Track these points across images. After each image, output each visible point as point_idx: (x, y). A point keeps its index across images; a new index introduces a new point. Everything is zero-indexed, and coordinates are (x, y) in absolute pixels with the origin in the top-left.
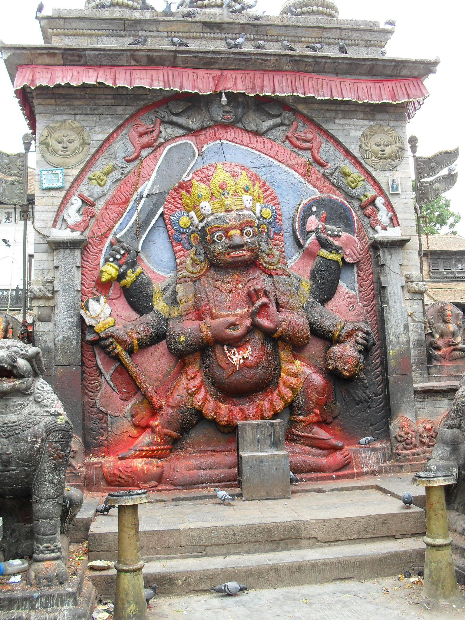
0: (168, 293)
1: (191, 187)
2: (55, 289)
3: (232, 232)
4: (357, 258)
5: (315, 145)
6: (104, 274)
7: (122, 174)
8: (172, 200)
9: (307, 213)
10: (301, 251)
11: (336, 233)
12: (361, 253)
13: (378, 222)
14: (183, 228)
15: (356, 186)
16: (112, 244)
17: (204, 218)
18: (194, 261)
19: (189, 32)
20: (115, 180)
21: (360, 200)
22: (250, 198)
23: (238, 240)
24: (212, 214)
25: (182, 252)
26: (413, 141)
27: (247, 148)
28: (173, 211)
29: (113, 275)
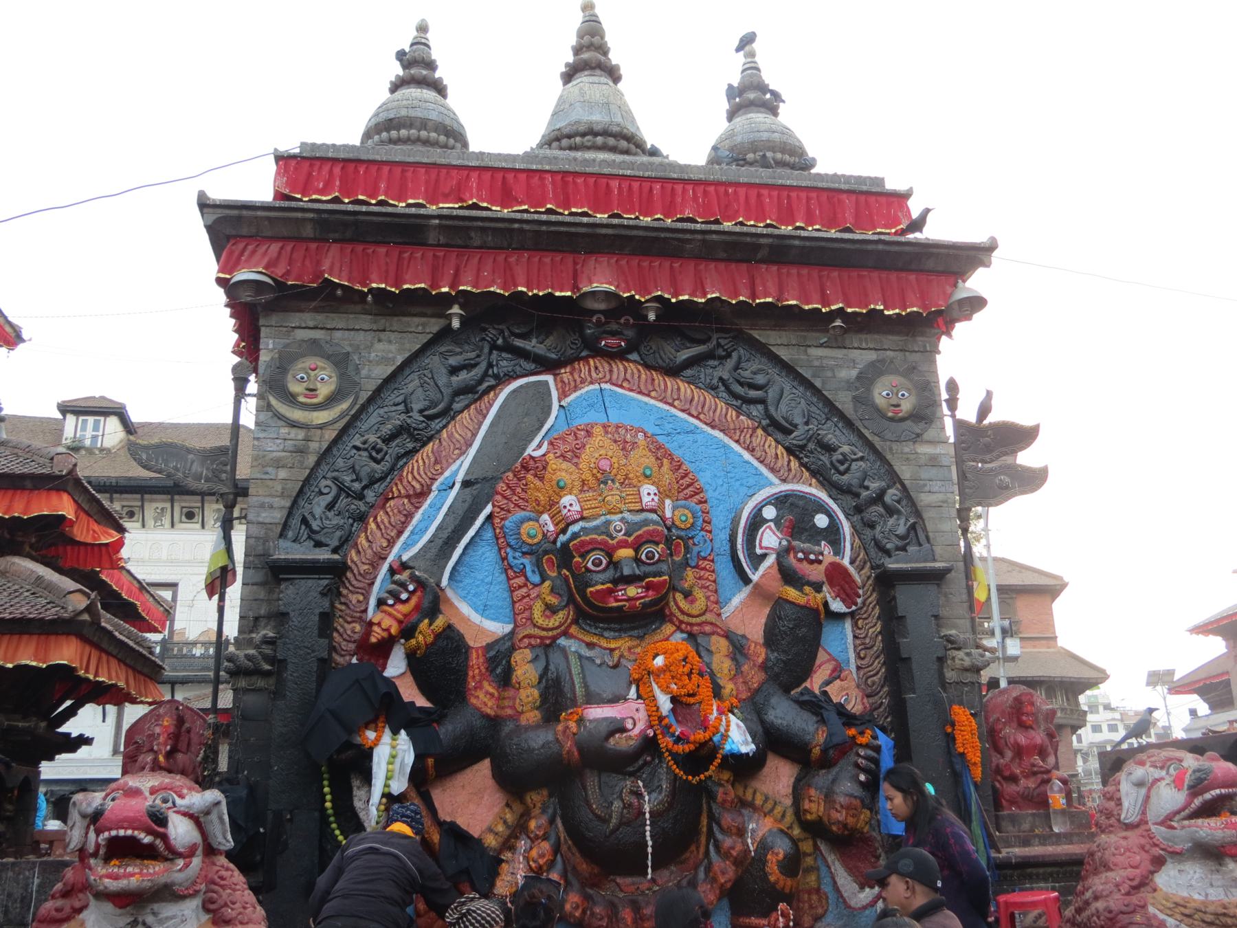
1: (544, 468)
5: (772, 394)
6: (376, 628)
7: (416, 440)
8: (508, 492)
10: (747, 590)
11: (812, 557)
12: (861, 592)
15: (848, 470)
16: (392, 571)
17: (568, 525)
20: (402, 451)
21: (857, 495)
22: (653, 489)
24: (582, 518)
25: (524, 590)
26: (952, 386)
27: (646, 399)
28: (509, 511)
29: (393, 631)
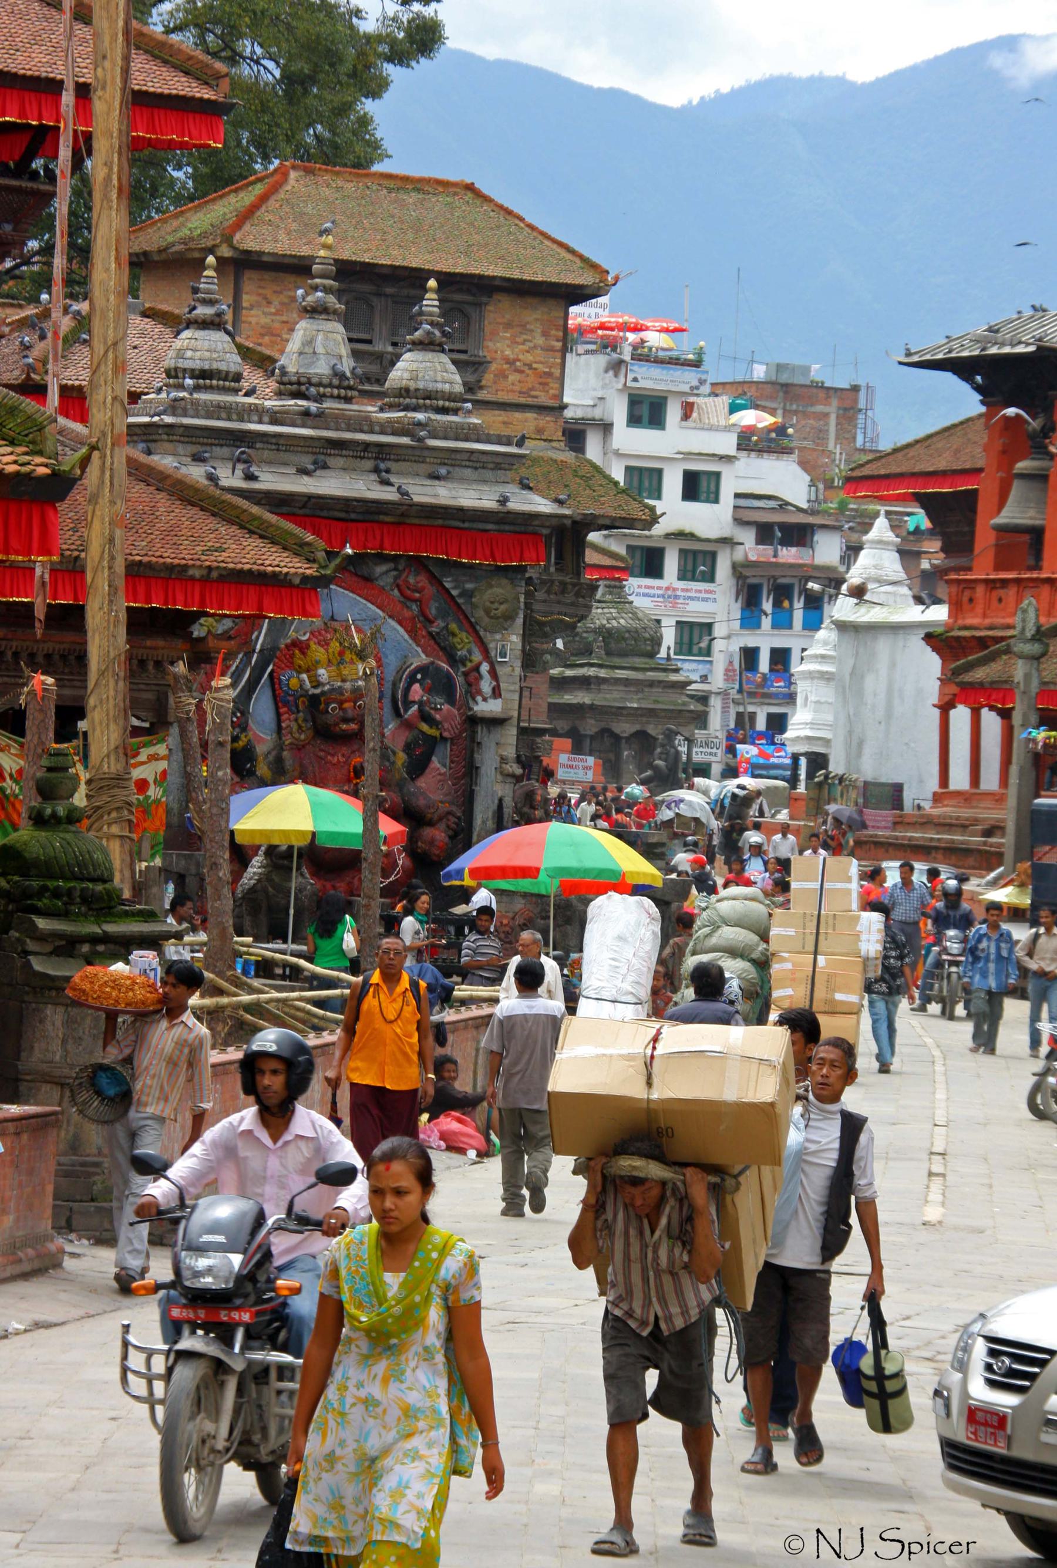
0: (271, 758)
3: (346, 705)
9: (412, 679)
13: (479, 692)
18: (300, 727)
23: (350, 714)
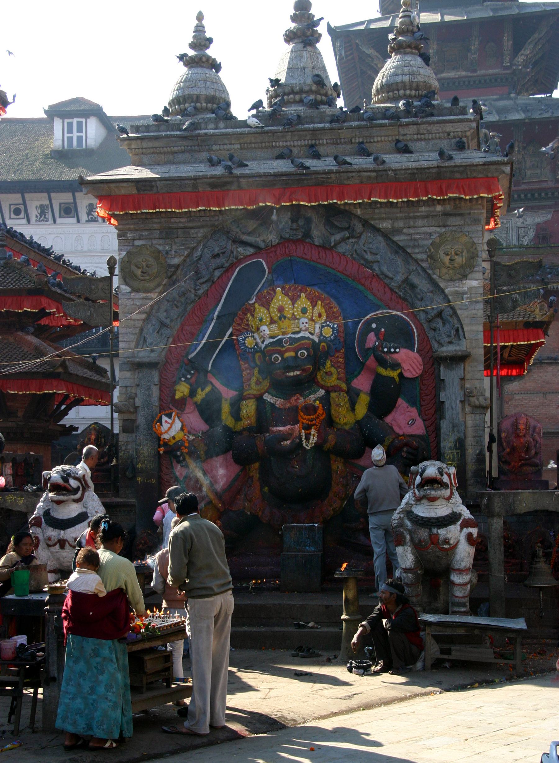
2: (137, 405)
4: (417, 373)
6: (177, 392)
11: (392, 350)
14: (249, 348)
19: (261, 143)
24: (271, 337)
29: (185, 394)
